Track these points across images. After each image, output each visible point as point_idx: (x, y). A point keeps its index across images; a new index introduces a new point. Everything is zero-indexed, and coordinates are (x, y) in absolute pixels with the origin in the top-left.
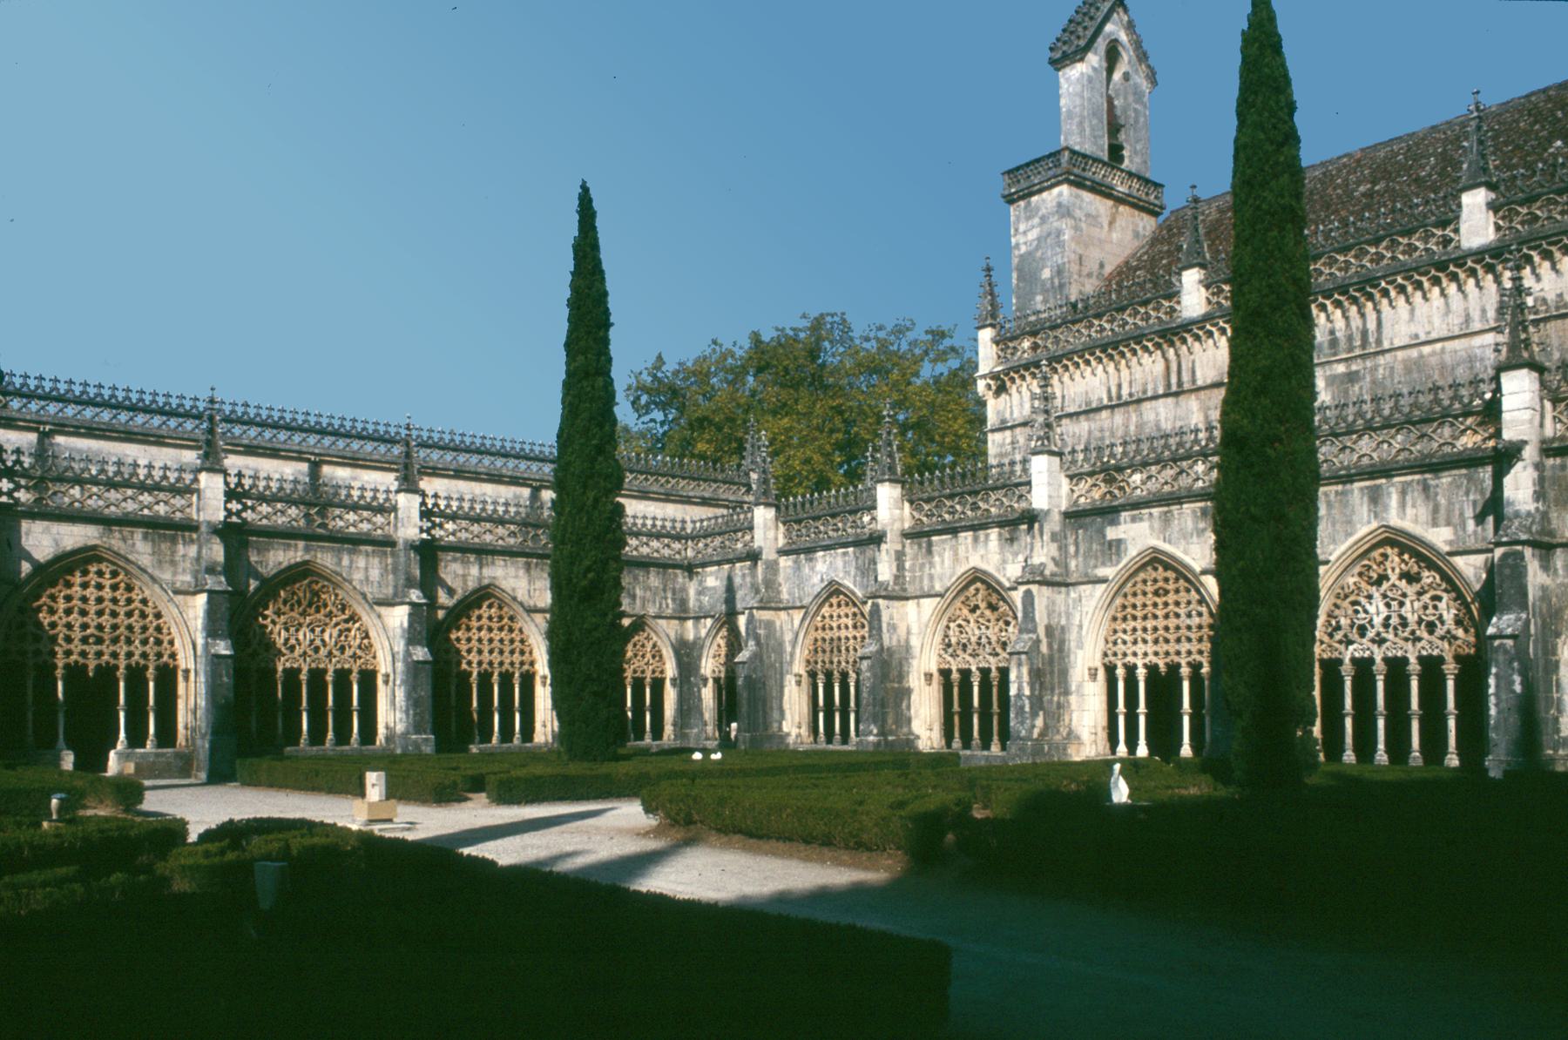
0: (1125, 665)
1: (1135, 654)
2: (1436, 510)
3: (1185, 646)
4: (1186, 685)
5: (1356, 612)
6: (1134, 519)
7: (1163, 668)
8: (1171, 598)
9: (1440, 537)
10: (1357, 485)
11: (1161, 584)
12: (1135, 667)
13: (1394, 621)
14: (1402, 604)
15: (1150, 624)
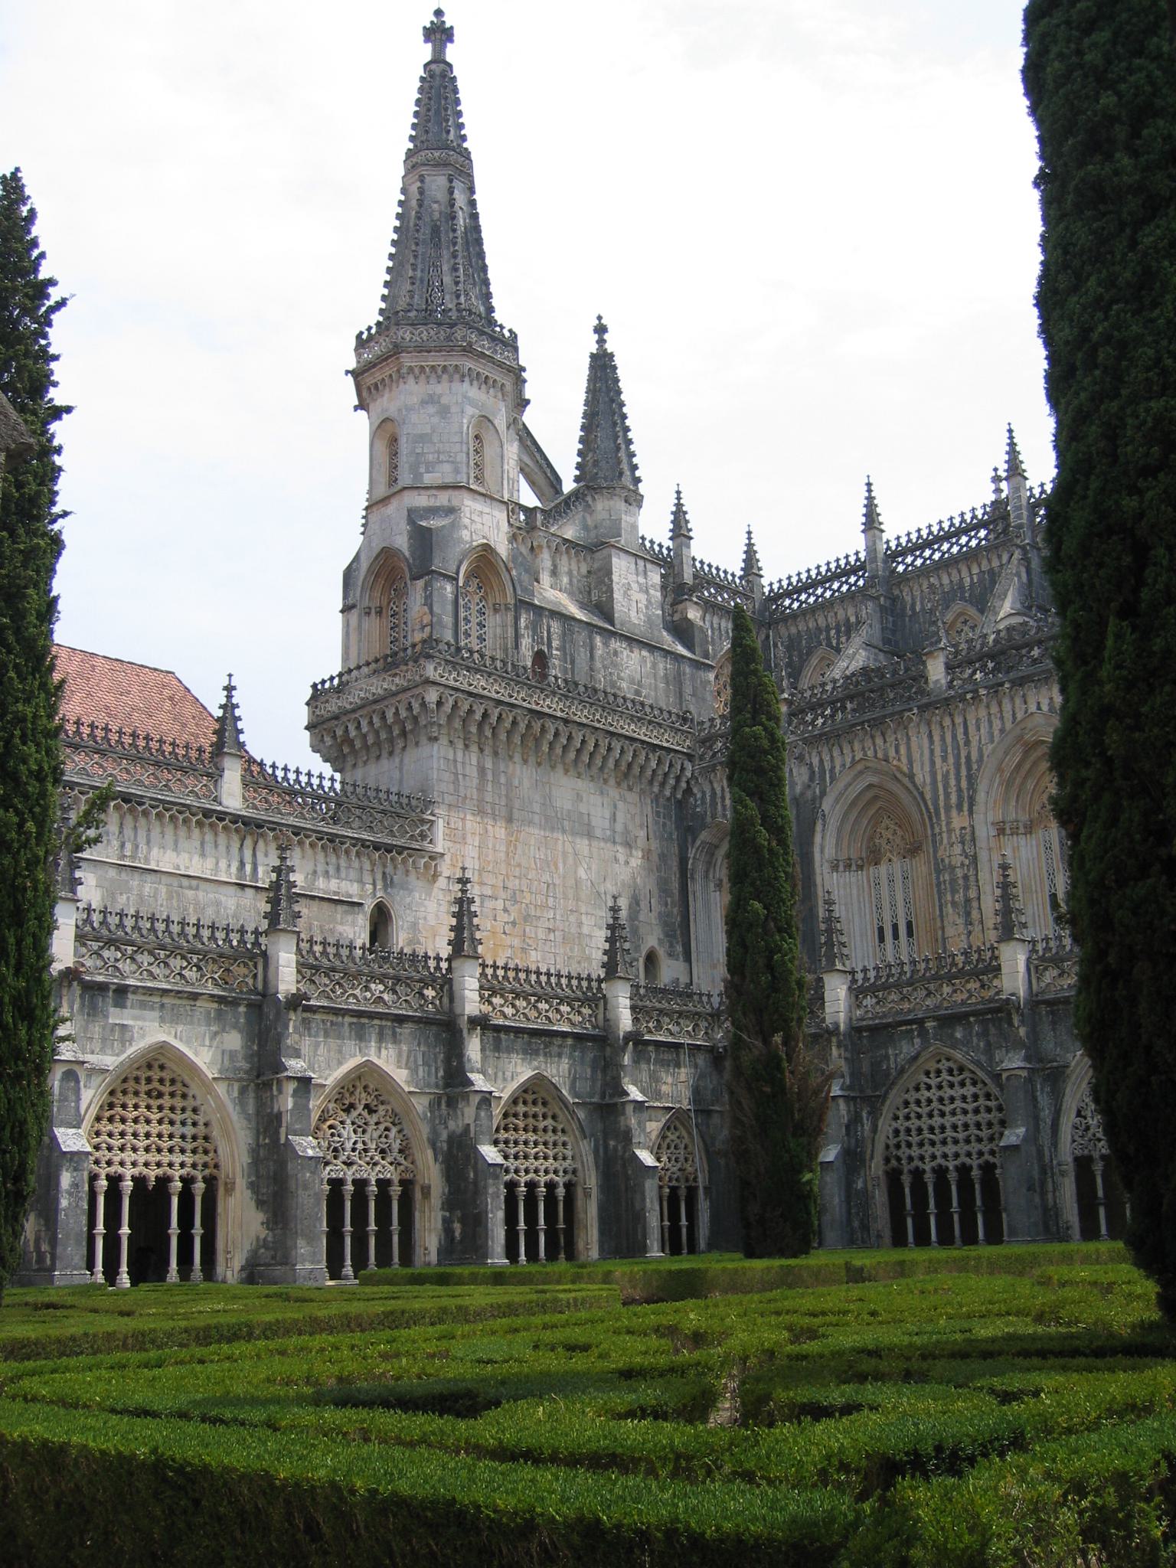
0: (108, 1177)
1: (122, 1164)
2: (400, 1054)
3: (177, 1158)
4: (372, 1205)
5: (333, 1135)
6: (143, 1005)
7: (152, 1183)
8: (167, 1101)
9: (400, 1076)
10: (348, 1019)
11: (156, 1084)
12: (119, 1178)
13: (360, 1146)
14: (364, 1132)
15: (142, 1128)
